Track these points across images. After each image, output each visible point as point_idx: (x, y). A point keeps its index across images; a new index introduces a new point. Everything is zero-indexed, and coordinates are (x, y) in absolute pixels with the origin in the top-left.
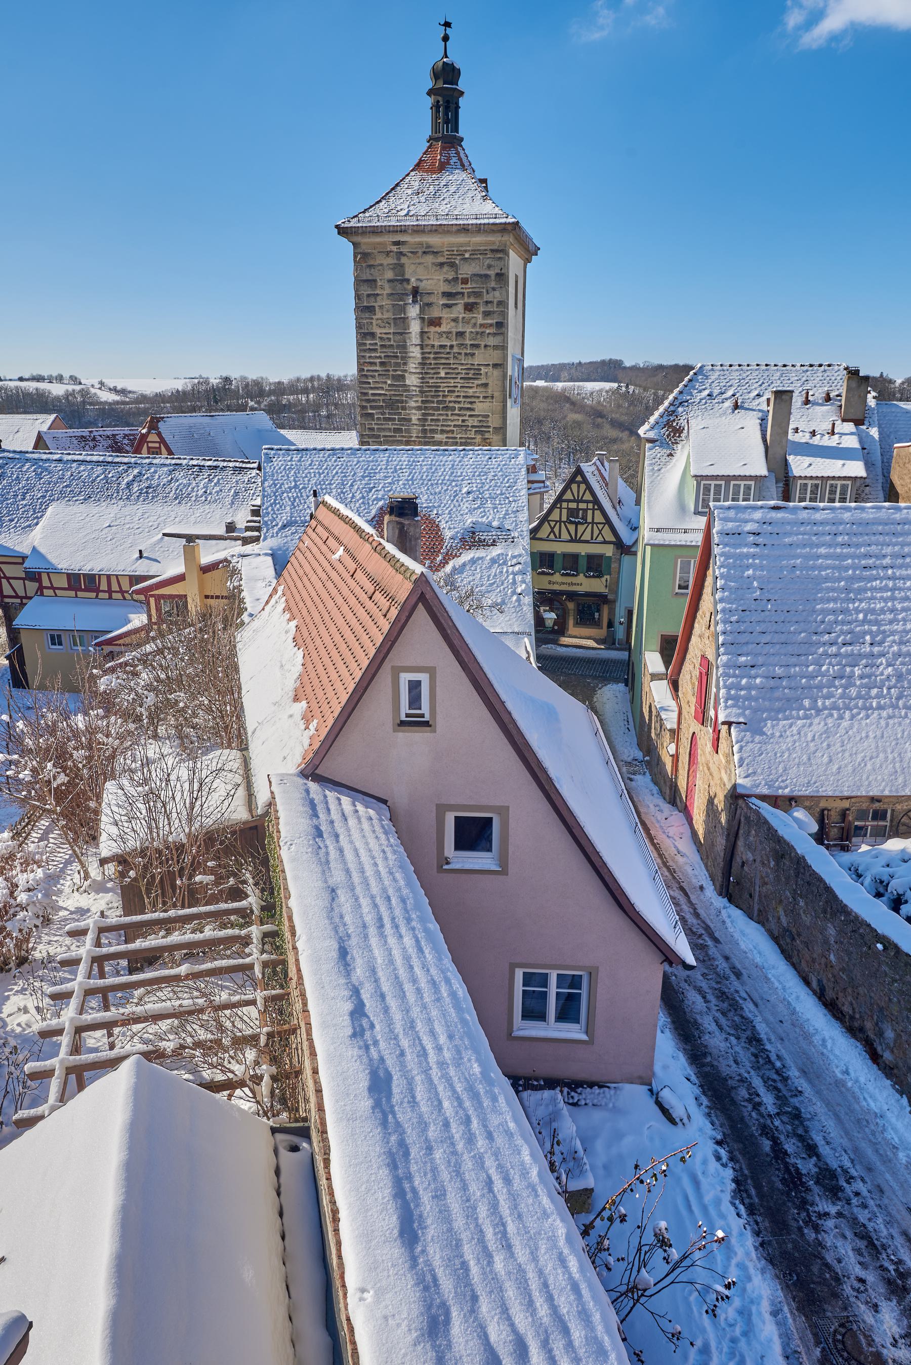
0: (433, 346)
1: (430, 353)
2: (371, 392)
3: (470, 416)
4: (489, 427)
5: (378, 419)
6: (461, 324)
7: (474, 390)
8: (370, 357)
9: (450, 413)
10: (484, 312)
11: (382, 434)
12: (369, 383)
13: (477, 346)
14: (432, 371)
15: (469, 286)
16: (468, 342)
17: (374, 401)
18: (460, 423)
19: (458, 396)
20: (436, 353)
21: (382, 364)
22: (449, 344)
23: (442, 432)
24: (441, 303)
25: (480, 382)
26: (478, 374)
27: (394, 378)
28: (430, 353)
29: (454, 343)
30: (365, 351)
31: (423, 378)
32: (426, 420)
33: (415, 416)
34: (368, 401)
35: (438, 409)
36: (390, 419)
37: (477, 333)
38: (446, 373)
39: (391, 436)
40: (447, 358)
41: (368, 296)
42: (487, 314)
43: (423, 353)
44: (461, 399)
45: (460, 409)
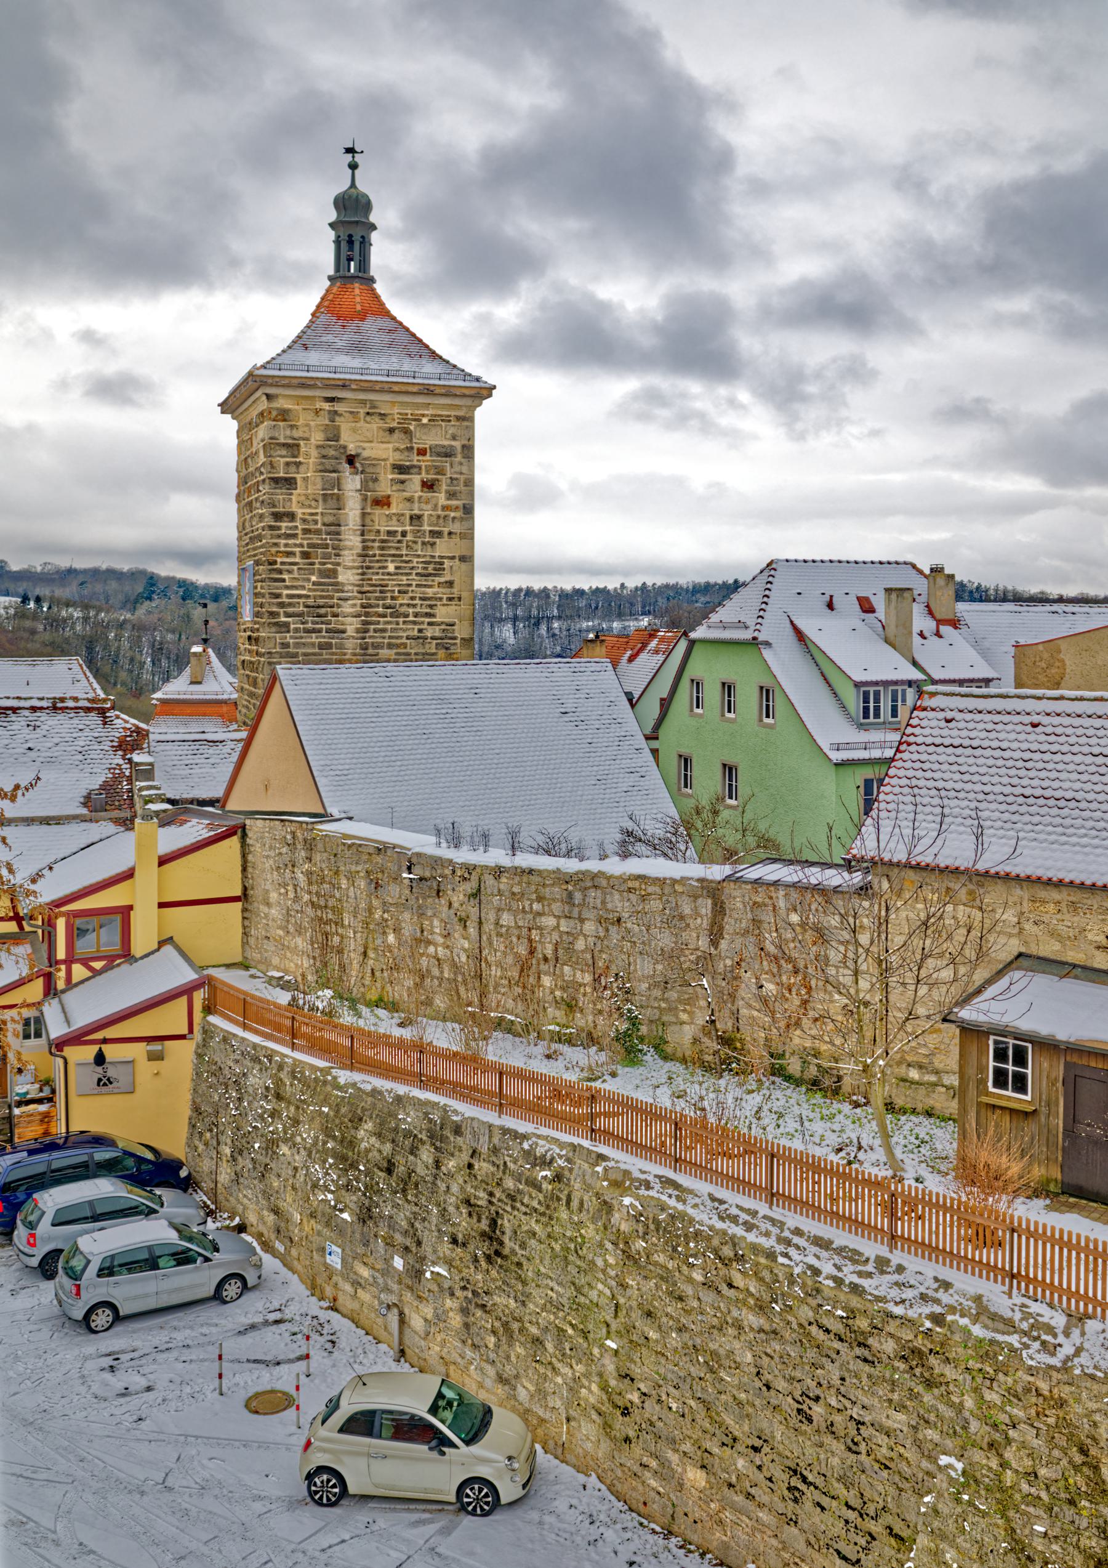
0: (378, 532)
1: (374, 541)
2: (285, 592)
3: (430, 624)
4: (455, 638)
5: (297, 630)
6: (416, 505)
7: (435, 590)
8: (286, 545)
9: (401, 620)
10: (447, 492)
11: (300, 651)
12: (284, 580)
13: (437, 534)
14: (377, 565)
15: (428, 457)
16: (426, 528)
17: (290, 605)
18: (416, 633)
19: (412, 598)
20: (383, 541)
21: (305, 555)
22: (400, 529)
23: (390, 646)
24: (390, 477)
25: (442, 580)
26: (439, 568)
27: (324, 573)
28: (374, 541)
29: (408, 528)
30: (279, 537)
31: (363, 574)
32: (367, 631)
33: (352, 626)
34: (282, 605)
35: (385, 616)
36: (314, 631)
37: (439, 517)
38: (397, 568)
39: (314, 654)
40: (398, 548)
41: (287, 464)
42: (451, 495)
43: (364, 541)
44: (417, 602)
45: (416, 615)
